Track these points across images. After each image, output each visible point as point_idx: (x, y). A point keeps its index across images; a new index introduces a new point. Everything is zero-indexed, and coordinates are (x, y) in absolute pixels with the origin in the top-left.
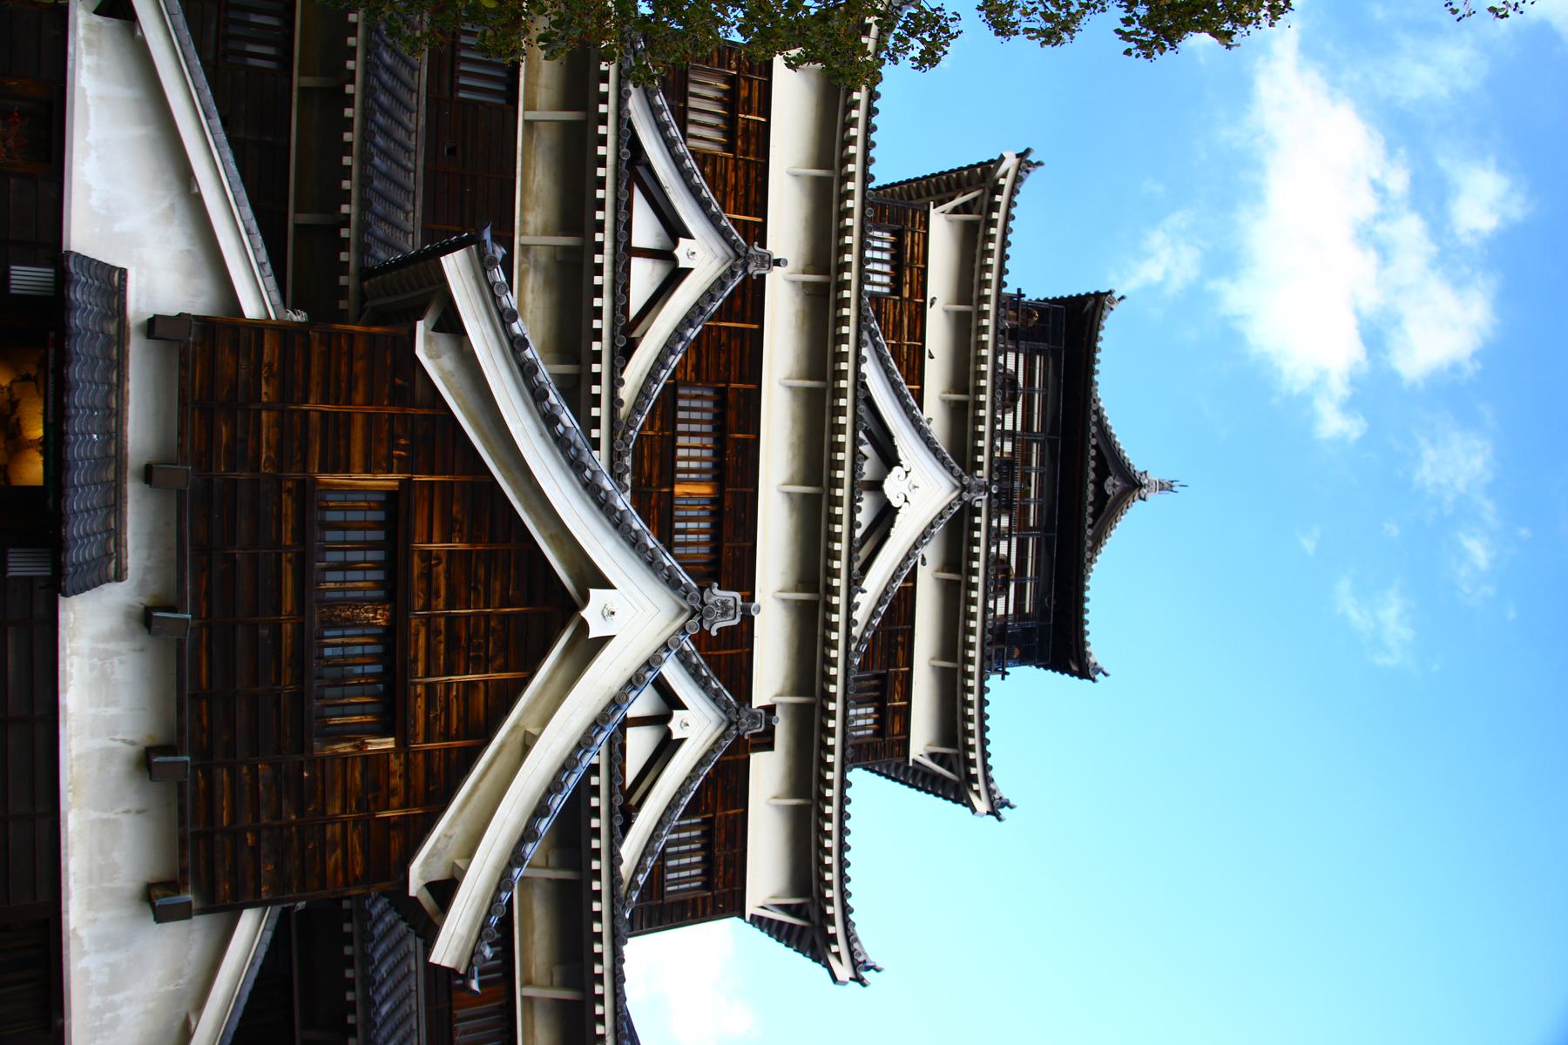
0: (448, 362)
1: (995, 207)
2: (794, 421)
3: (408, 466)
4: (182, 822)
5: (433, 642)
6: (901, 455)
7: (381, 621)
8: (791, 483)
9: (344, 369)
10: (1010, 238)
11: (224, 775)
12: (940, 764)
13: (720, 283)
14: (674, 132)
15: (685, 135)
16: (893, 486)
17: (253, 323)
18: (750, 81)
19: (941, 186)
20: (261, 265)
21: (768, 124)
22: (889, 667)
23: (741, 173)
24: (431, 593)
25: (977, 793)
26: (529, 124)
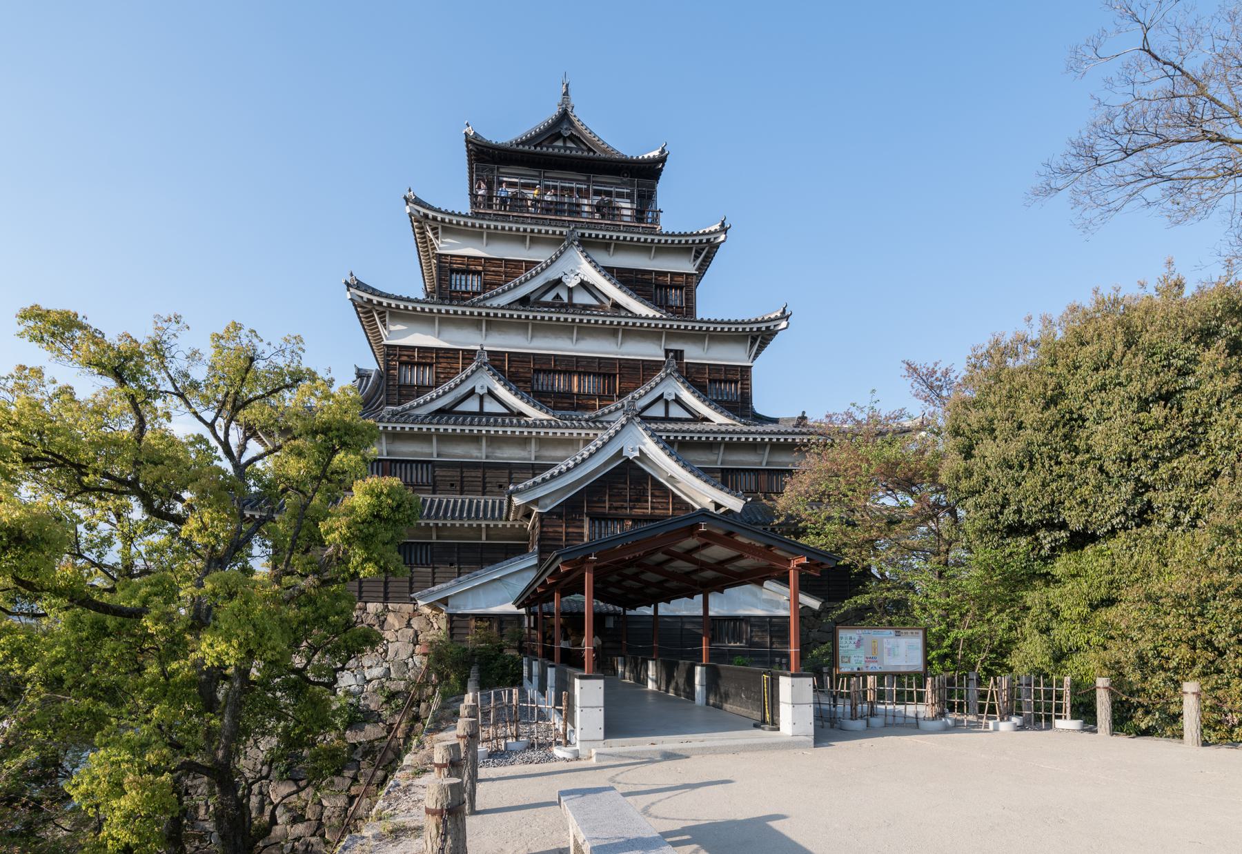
0: (548, 501)
2: (546, 337)
3: (581, 514)
6: (557, 277)
8: (572, 339)
15: (430, 388)
16: (572, 282)
19: (423, 243)
21: (420, 348)
24: (622, 507)
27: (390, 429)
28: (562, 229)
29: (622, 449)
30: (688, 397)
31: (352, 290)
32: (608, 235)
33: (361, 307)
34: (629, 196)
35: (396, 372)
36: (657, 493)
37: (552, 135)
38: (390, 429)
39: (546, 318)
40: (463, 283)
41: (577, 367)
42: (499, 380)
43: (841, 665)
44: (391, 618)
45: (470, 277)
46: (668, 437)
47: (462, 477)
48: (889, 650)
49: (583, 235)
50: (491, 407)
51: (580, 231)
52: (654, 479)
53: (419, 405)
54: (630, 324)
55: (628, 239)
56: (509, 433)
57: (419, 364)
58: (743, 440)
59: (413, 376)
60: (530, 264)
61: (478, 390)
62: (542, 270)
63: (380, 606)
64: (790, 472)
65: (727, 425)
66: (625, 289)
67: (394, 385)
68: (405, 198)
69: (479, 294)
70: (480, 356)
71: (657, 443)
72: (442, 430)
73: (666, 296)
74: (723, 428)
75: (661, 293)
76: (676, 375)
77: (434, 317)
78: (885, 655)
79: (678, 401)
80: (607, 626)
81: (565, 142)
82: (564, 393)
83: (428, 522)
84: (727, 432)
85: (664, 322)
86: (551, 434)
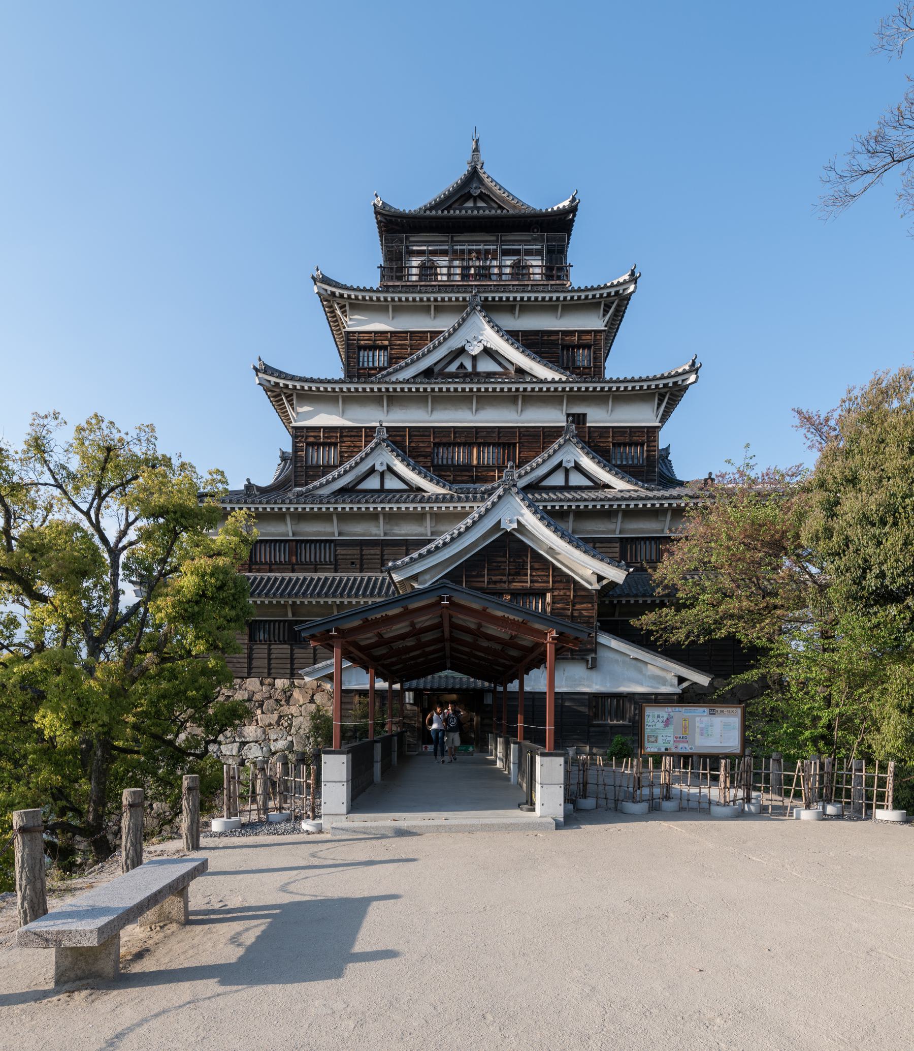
0: (427, 577)
2: (446, 409)
6: (460, 346)
7: (509, 597)
10: (355, 287)
12: (608, 312)
14: (335, 473)
16: (475, 350)
19: (334, 322)
21: (325, 428)
22: (558, 344)
24: (501, 581)
25: (624, 290)
27: (292, 510)
28: (464, 295)
29: (500, 521)
30: (587, 463)
31: (260, 375)
32: (511, 296)
33: (271, 391)
34: (538, 253)
35: (303, 454)
36: (537, 566)
37: (461, 196)
38: (292, 510)
39: (452, 390)
40: (371, 359)
41: (477, 438)
42: (398, 456)
43: (646, 745)
44: (296, 694)
45: (377, 353)
46: (545, 507)
47: (362, 555)
48: (702, 729)
49: (486, 299)
50: (392, 483)
51: (483, 295)
52: (534, 551)
53: (322, 486)
54: (529, 389)
55: (533, 299)
56: (403, 509)
57: (324, 444)
58: (641, 506)
61: (378, 467)
62: (445, 339)
63: (287, 682)
64: (668, 539)
65: (629, 491)
66: (528, 352)
67: (301, 467)
68: (313, 278)
69: (385, 369)
70: (379, 432)
71: (535, 513)
72: (340, 509)
73: (573, 357)
74: (627, 495)
75: (568, 354)
76: (575, 440)
77: (337, 396)
78: (697, 735)
79: (578, 468)
80: (486, 702)
81: (475, 202)
82: (464, 466)
83: (326, 600)
84: (631, 499)
85: (564, 385)
86: (443, 509)
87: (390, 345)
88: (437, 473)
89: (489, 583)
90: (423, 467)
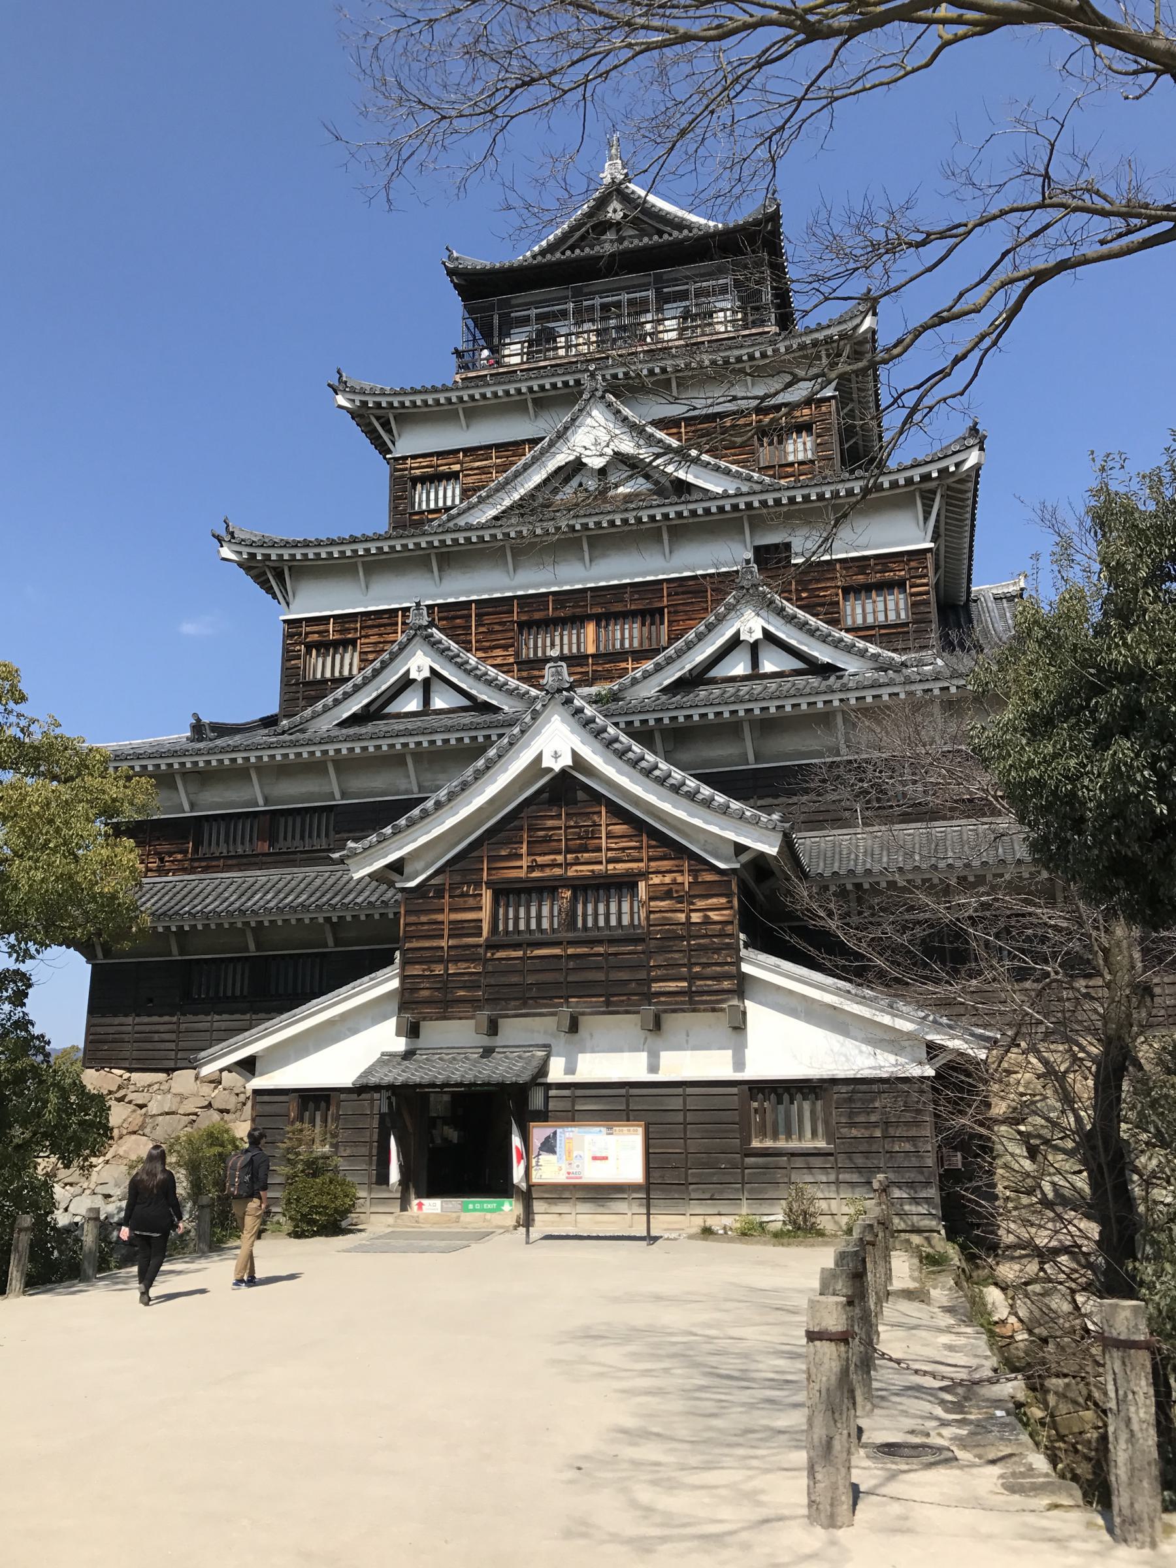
0: (419, 865)
1: (378, 405)
3: (478, 884)
4: (683, 1011)
5: (582, 860)
7: (569, 893)
8: (582, 559)
9: (426, 928)
11: (656, 987)
13: (434, 644)
14: (339, 693)
17: (402, 982)
18: (307, 634)
20: (372, 979)
23: (370, 632)
26: (344, 796)
59: (320, 667)
60: (534, 442)
87: (462, 471)
88: (525, 674)
89: (531, 868)
90: (493, 666)
